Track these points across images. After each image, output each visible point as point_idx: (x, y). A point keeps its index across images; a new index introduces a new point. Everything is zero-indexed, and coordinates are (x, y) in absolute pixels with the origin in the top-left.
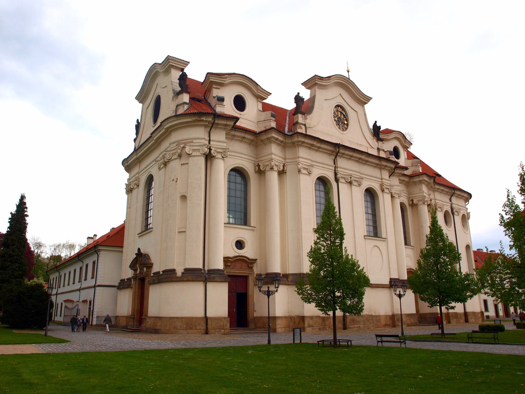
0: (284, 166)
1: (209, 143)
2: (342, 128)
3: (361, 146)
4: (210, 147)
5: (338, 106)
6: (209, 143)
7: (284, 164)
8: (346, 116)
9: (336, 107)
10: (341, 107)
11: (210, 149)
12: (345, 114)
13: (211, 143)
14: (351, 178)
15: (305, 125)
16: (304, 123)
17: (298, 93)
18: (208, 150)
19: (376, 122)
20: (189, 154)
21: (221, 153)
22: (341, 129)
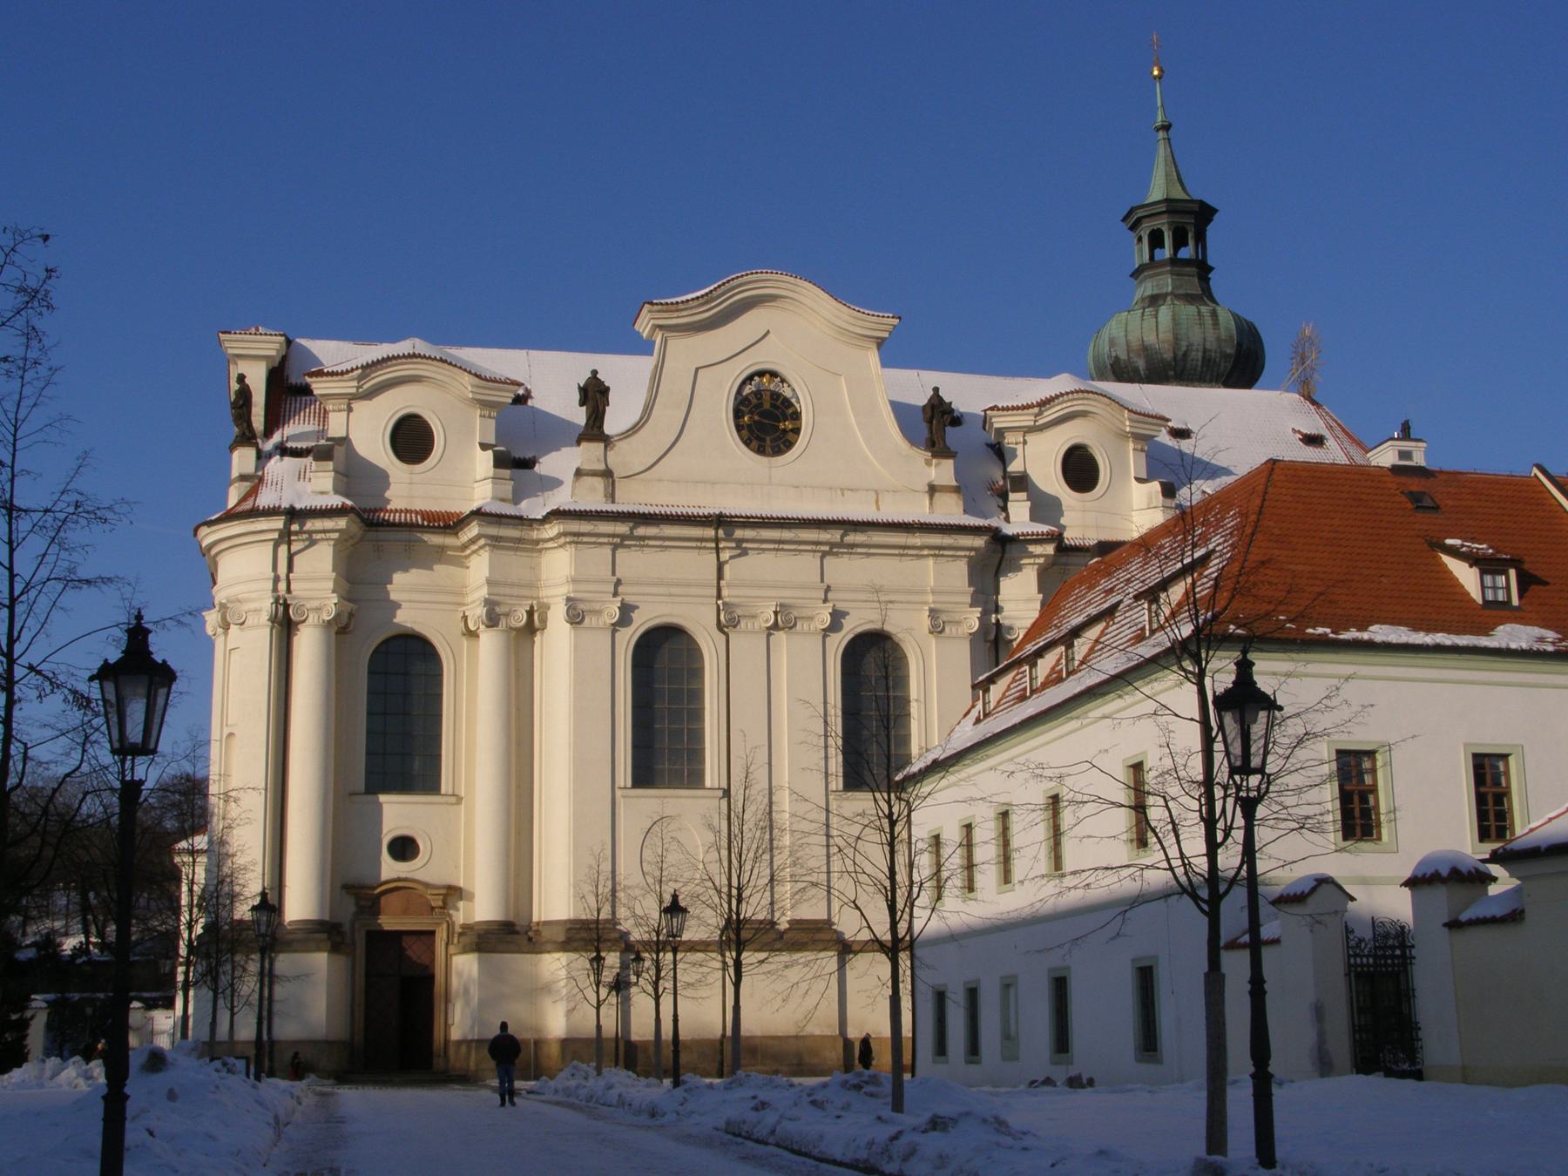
0: (530, 613)
1: (289, 590)
2: (773, 448)
3: (846, 492)
4: (285, 600)
5: (761, 374)
6: (289, 590)
7: (532, 607)
8: (793, 401)
9: (750, 378)
10: (773, 374)
11: (287, 606)
12: (787, 392)
13: (293, 586)
14: (776, 613)
15: (607, 474)
16: (602, 467)
17: (595, 373)
18: (281, 609)
19: (936, 390)
20: (243, 623)
21: (318, 609)
22: (769, 450)
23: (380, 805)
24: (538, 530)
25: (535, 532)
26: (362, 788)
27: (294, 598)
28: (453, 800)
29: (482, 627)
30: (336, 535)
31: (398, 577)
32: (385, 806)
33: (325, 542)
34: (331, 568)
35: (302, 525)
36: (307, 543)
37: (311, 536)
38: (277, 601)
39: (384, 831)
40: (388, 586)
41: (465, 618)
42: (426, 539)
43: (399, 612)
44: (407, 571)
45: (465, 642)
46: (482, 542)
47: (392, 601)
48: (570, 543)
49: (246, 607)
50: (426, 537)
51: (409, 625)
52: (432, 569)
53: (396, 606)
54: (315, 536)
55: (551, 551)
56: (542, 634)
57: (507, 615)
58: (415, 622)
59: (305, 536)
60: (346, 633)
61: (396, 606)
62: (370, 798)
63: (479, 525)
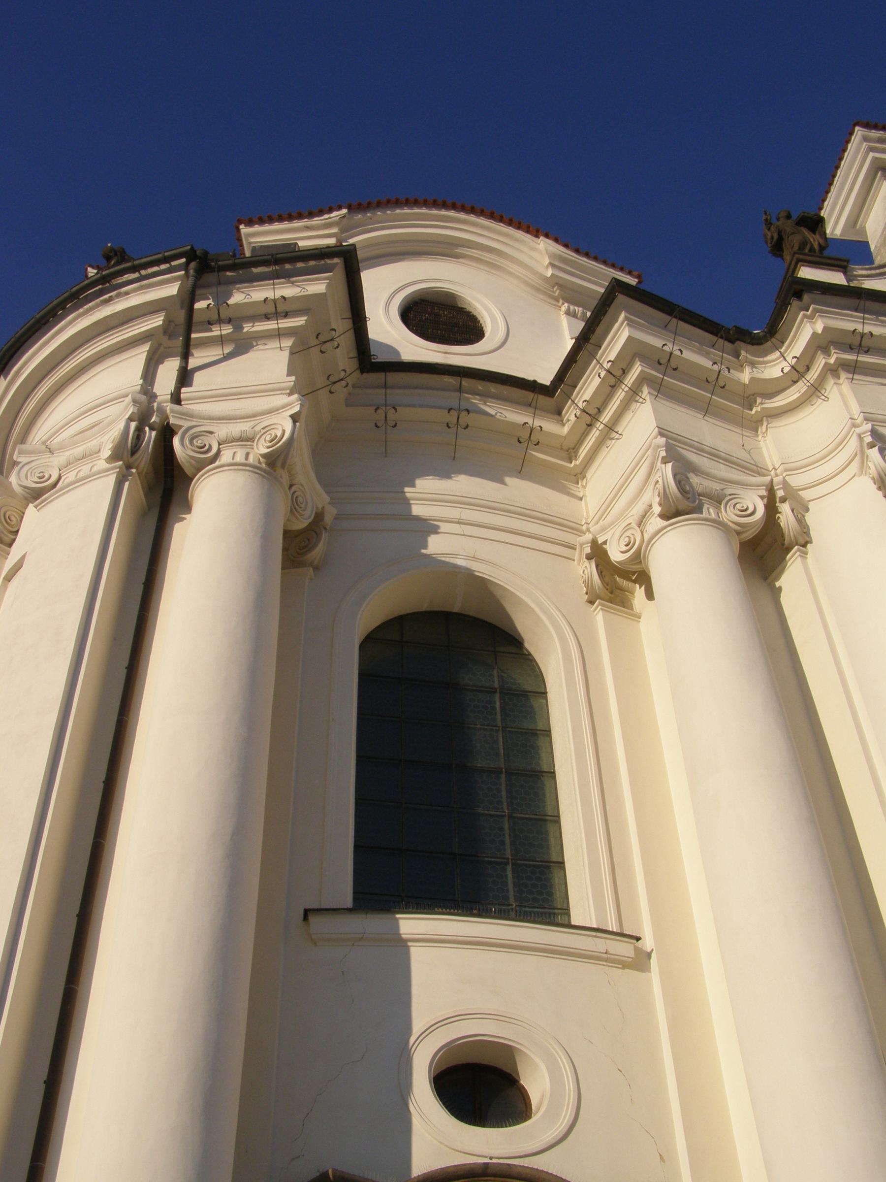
11: (167, 432)
18: (150, 436)
21: (246, 440)
23: (401, 946)
24: (753, 365)
25: (747, 370)
26: (349, 903)
27: (189, 415)
28: (624, 949)
29: (655, 523)
30: (299, 321)
31: (426, 485)
32: (418, 955)
33: (275, 344)
34: (285, 370)
35: (221, 300)
36: (228, 349)
37: (238, 328)
38: (142, 418)
39: (418, 1026)
40: (407, 489)
41: (598, 553)
42: (492, 412)
43: (432, 540)
44: (449, 477)
45: (599, 617)
46: (637, 370)
47: (418, 519)
48: (833, 371)
49: (59, 459)
50: (492, 408)
51: (460, 562)
52: (503, 483)
53: (427, 527)
54: (247, 328)
55: (776, 423)
56: (804, 555)
57: (718, 500)
58: (475, 559)
59: (227, 330)
60: (302, 564)
61: (427, 527)
62: (373, 923)
63: (631, 324)
